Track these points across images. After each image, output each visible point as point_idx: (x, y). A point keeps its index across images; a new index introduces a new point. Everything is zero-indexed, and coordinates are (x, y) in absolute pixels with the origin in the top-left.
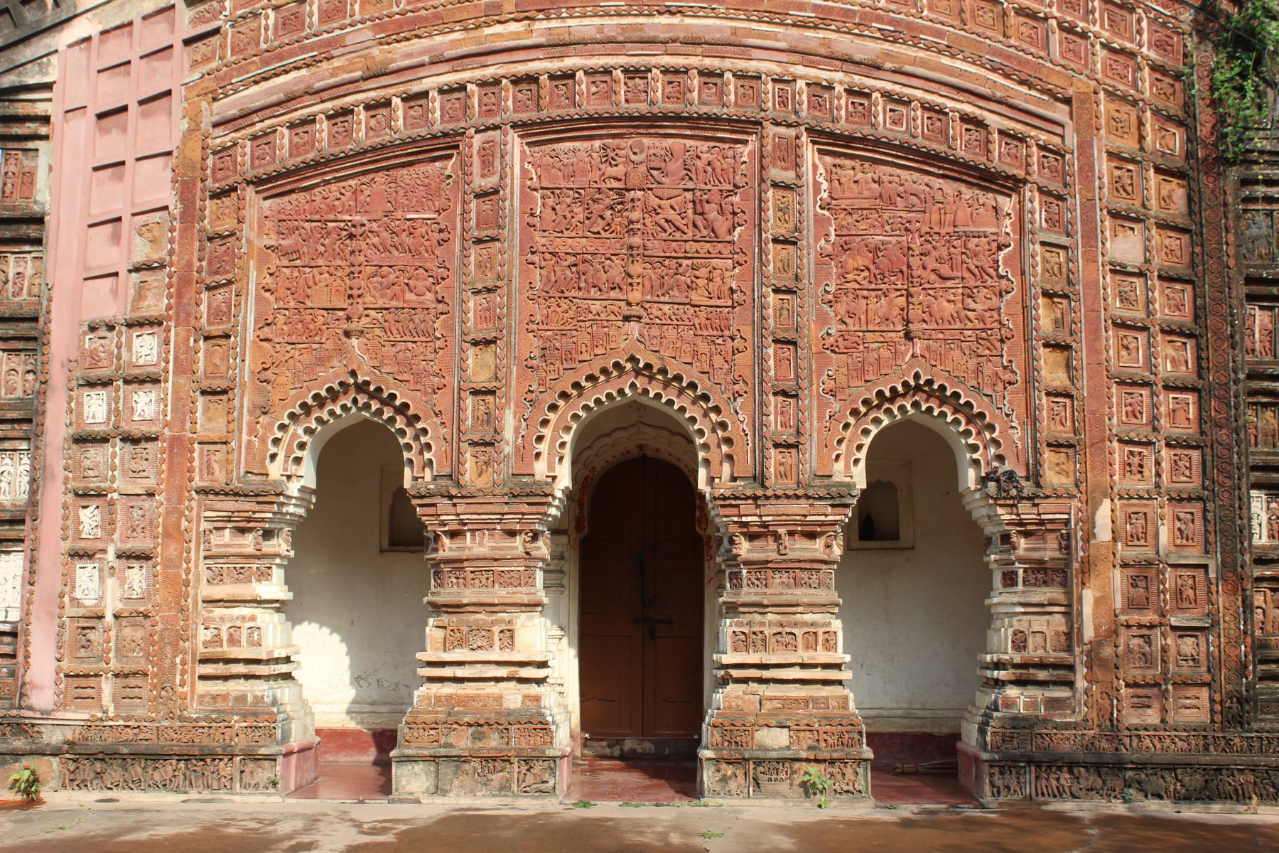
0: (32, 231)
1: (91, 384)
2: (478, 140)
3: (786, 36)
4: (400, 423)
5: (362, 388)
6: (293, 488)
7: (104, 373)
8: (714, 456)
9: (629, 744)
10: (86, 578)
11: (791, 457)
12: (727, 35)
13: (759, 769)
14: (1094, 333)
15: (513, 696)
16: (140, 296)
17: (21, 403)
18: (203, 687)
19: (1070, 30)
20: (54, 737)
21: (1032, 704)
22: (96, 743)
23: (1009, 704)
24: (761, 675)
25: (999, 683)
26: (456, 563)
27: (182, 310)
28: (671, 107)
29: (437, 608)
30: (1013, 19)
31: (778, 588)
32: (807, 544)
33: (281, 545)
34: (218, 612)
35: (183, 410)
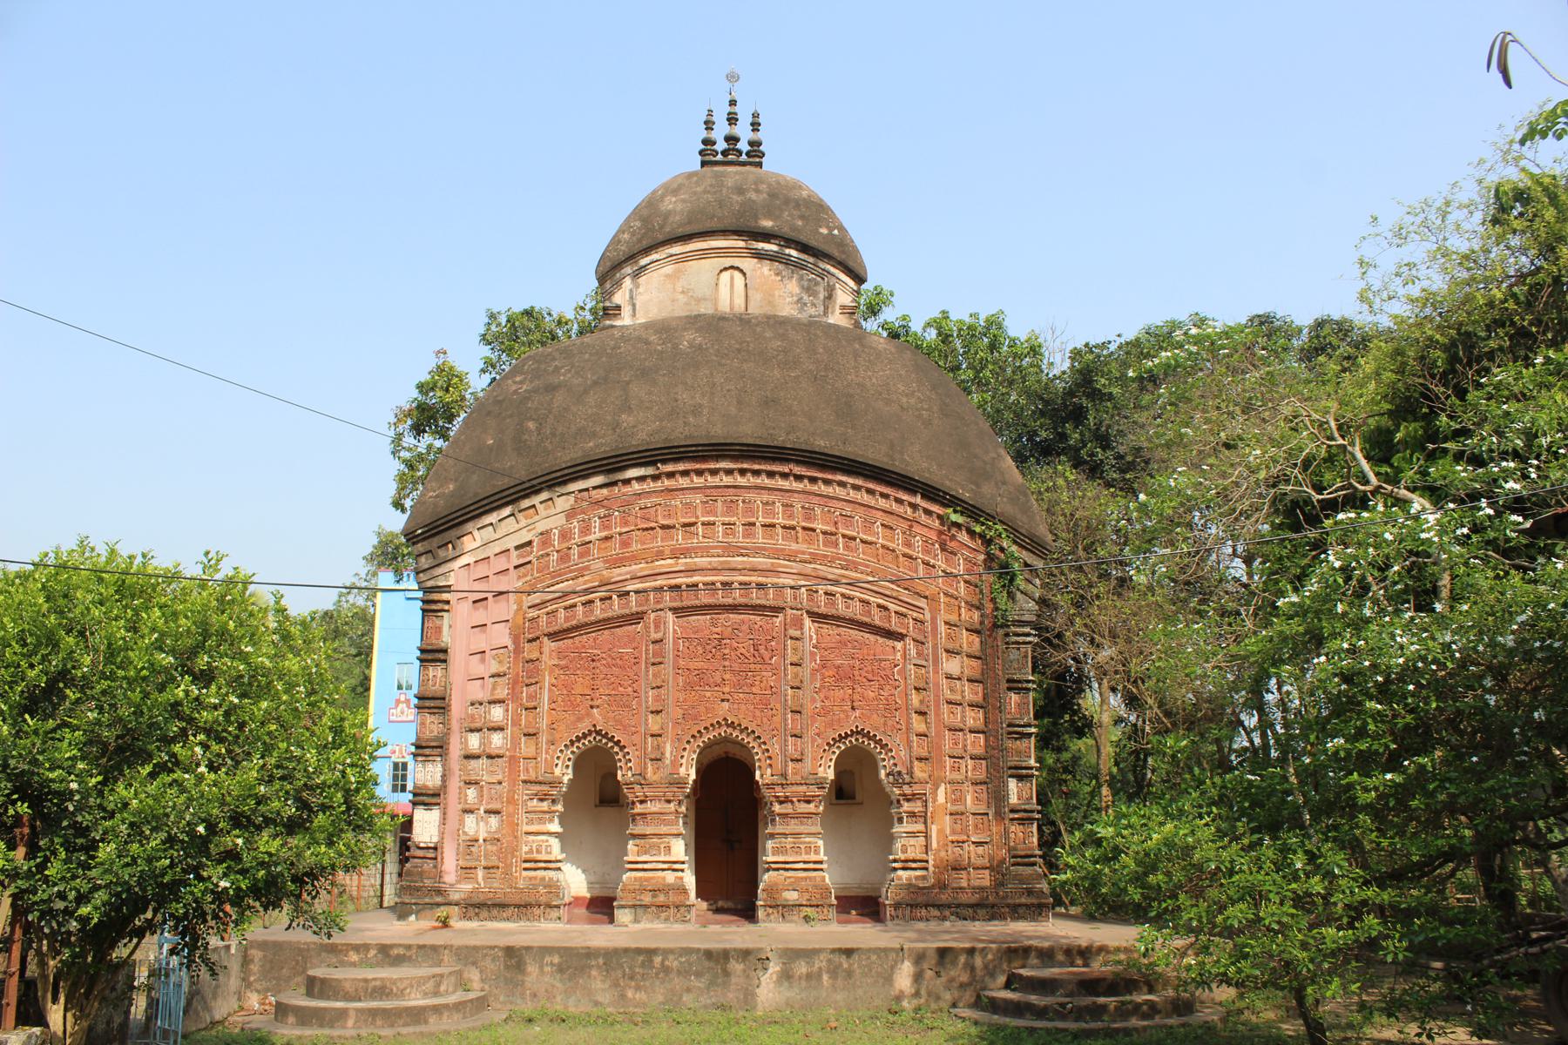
0: (441, 656)
1: (472, 731)
2: (653, 616)
3: (796, 567)
4: (616, 749)
5: (598, 733)
6: (566, 779)
7: (478, 725)
8: (763, 764)
9: (720, 903)
10: (470, 820)
11: (798, 765)
12: (769, 567)
13: (784, 909)
14: (937, 706)
15: (670, 877)
16: (494, 688)
17: (436, 739)
18: (525, 873)
19: (927, 564)
20: (455, 897)
21: (909, 879)
22: (476, 900)
23: (900, 878)
24: (784, 867)
25: (895, 869)
26: (643, 815)
27: (515, 695)
28: (743, 600)
29: (634, 836)
30: (901, 559)
31: (793, 826)
32: (804, 805)
33: (560, 807)
34: (531, 838)
35: (515, 743)
